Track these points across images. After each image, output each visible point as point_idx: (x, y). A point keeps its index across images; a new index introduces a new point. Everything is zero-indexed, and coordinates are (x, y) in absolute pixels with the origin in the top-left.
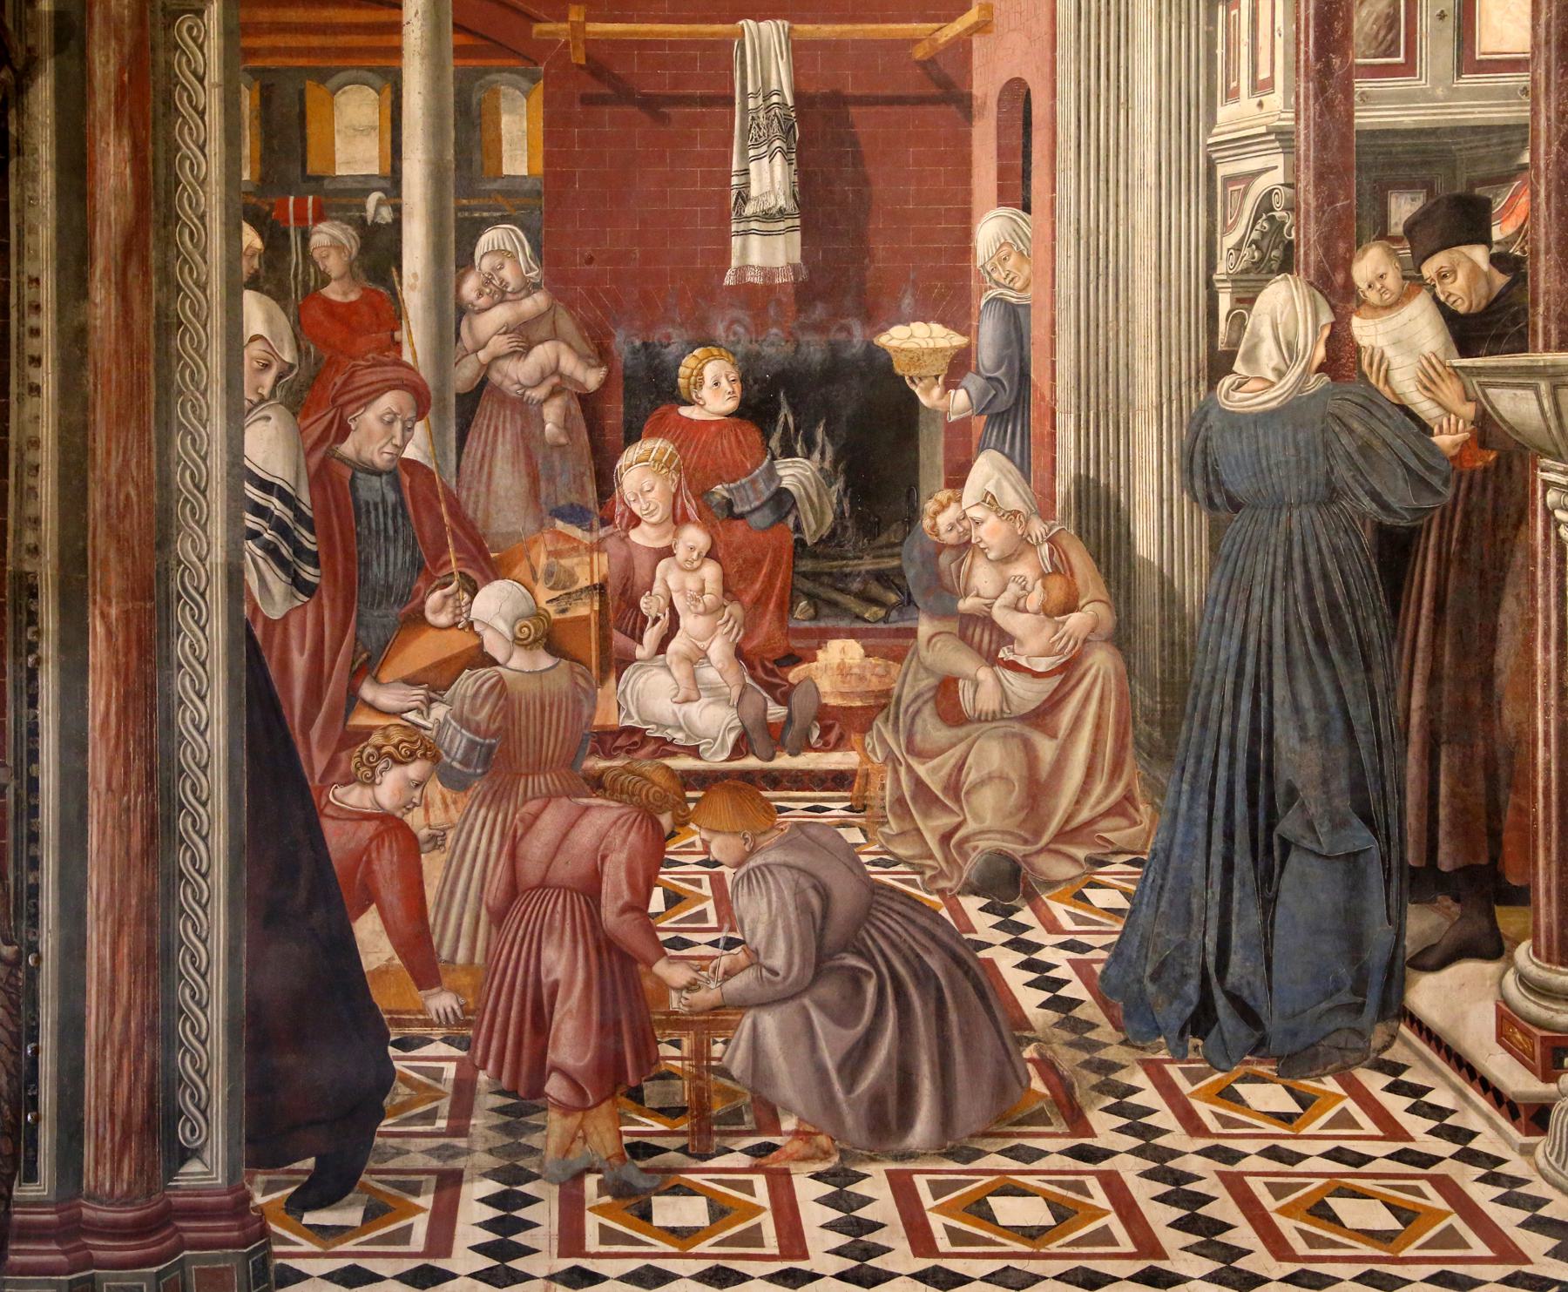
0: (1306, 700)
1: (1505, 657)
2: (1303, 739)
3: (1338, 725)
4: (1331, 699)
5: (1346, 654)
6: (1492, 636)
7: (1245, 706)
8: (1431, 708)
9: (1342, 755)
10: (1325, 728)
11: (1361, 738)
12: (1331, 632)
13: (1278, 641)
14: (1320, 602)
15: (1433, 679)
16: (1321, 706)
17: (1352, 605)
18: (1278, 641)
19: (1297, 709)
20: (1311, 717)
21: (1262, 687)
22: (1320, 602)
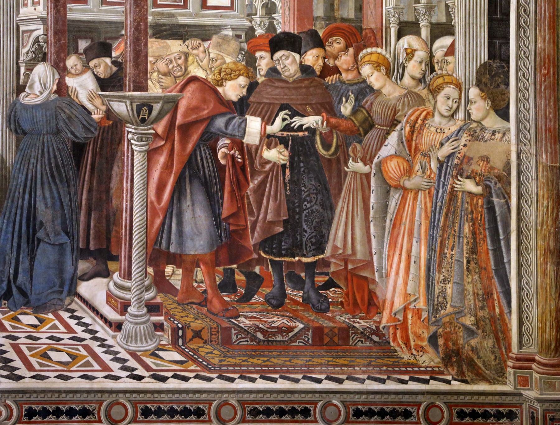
0: (48, 195)
1: (114, 184)
2: (46, 207)
3: (58, 203)
4: (56, 195)
5: (61, 181)
6: (110, 178)
7: (27, 196)
8: (89, 199)
9: (59, 214)
10: (54, 204)
11: (65, 207)
12: (56, 174)
13: (39, 176)
14: (53, 165)
15: (90, 191)
16: (53, 198)
17: (64, 166)
18: (39, 176)
19: (44, 198)
20: (49, 201)
21: (33, 190)
22: (53, 165)
